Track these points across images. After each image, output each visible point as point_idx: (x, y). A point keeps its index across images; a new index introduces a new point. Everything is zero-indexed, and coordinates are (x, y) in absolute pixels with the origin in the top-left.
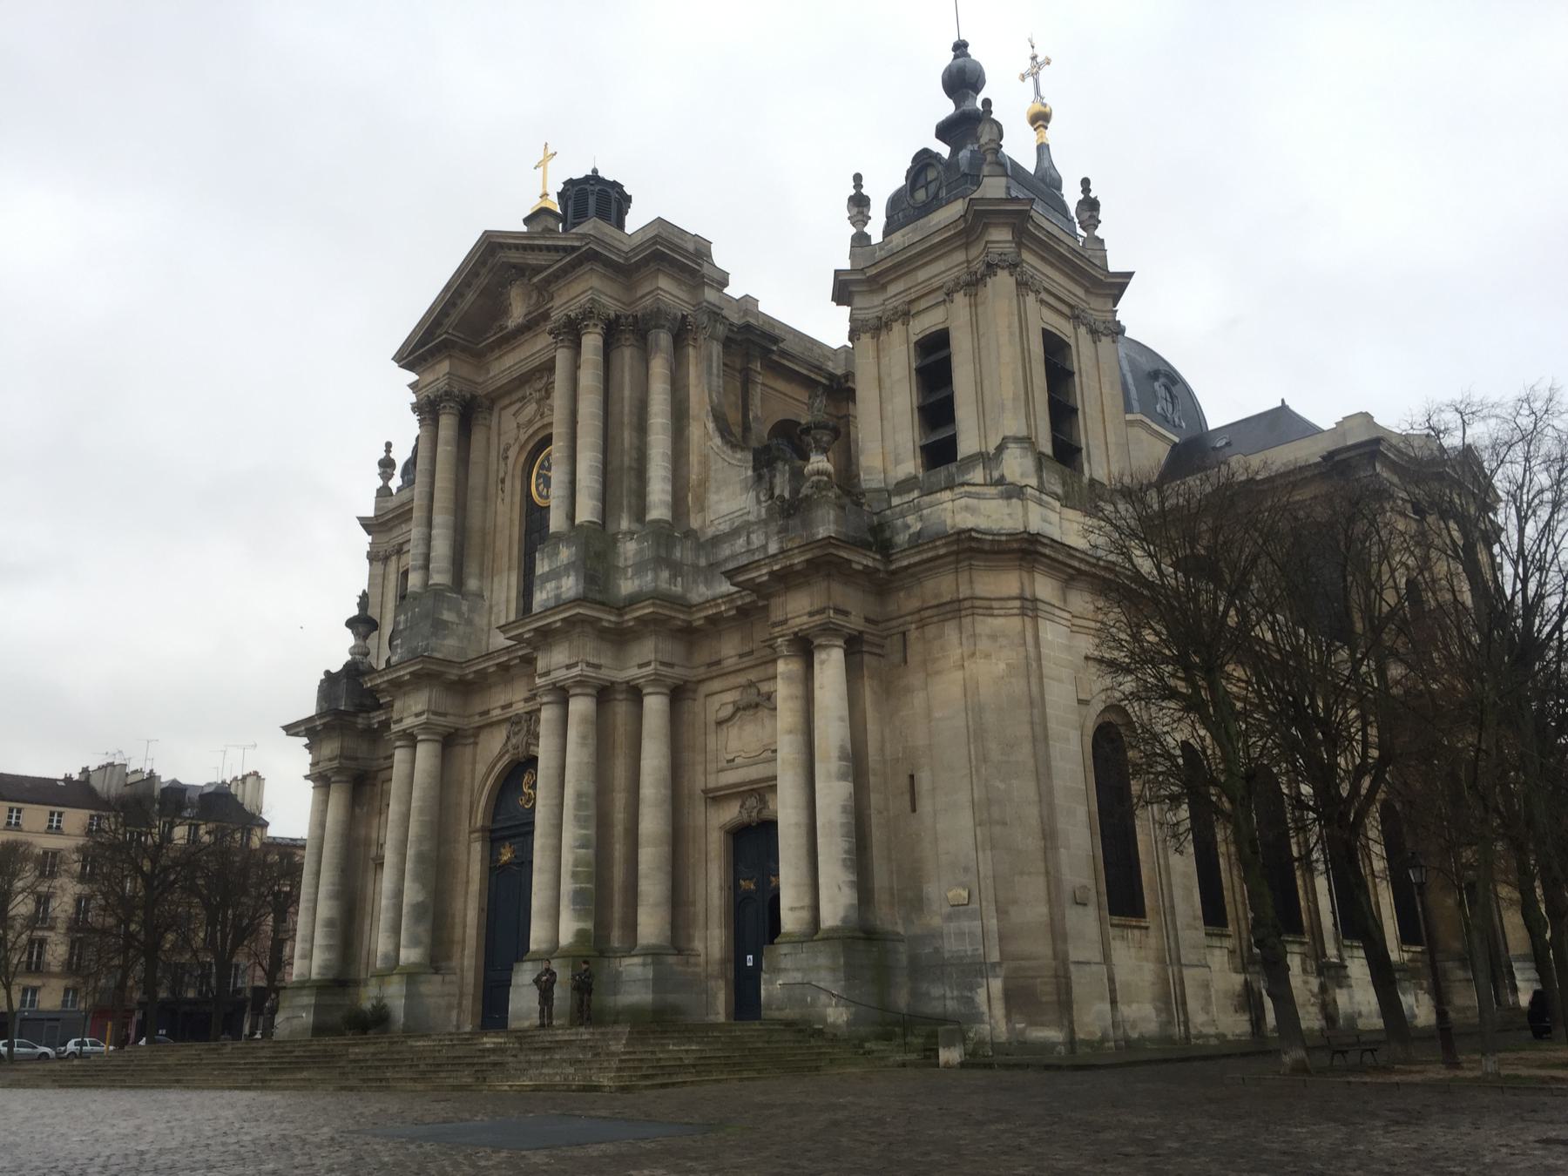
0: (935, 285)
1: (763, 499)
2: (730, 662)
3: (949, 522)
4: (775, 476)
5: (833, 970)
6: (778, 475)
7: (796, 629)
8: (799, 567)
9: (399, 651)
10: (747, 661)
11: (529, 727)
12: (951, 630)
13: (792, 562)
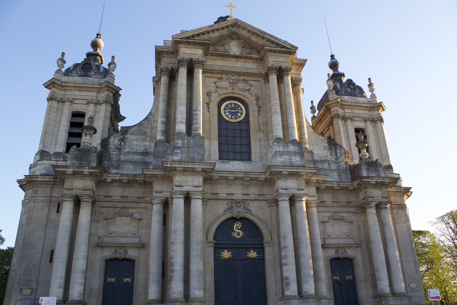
0: (361, 116)
1: (333, 155)
2: (329, 203)
4: (337, 150)
6: (338, 149)
7: (381, 201)
8: (386, 183)
9: (179, 155)
10: (336, 204)
13: (385, 181)
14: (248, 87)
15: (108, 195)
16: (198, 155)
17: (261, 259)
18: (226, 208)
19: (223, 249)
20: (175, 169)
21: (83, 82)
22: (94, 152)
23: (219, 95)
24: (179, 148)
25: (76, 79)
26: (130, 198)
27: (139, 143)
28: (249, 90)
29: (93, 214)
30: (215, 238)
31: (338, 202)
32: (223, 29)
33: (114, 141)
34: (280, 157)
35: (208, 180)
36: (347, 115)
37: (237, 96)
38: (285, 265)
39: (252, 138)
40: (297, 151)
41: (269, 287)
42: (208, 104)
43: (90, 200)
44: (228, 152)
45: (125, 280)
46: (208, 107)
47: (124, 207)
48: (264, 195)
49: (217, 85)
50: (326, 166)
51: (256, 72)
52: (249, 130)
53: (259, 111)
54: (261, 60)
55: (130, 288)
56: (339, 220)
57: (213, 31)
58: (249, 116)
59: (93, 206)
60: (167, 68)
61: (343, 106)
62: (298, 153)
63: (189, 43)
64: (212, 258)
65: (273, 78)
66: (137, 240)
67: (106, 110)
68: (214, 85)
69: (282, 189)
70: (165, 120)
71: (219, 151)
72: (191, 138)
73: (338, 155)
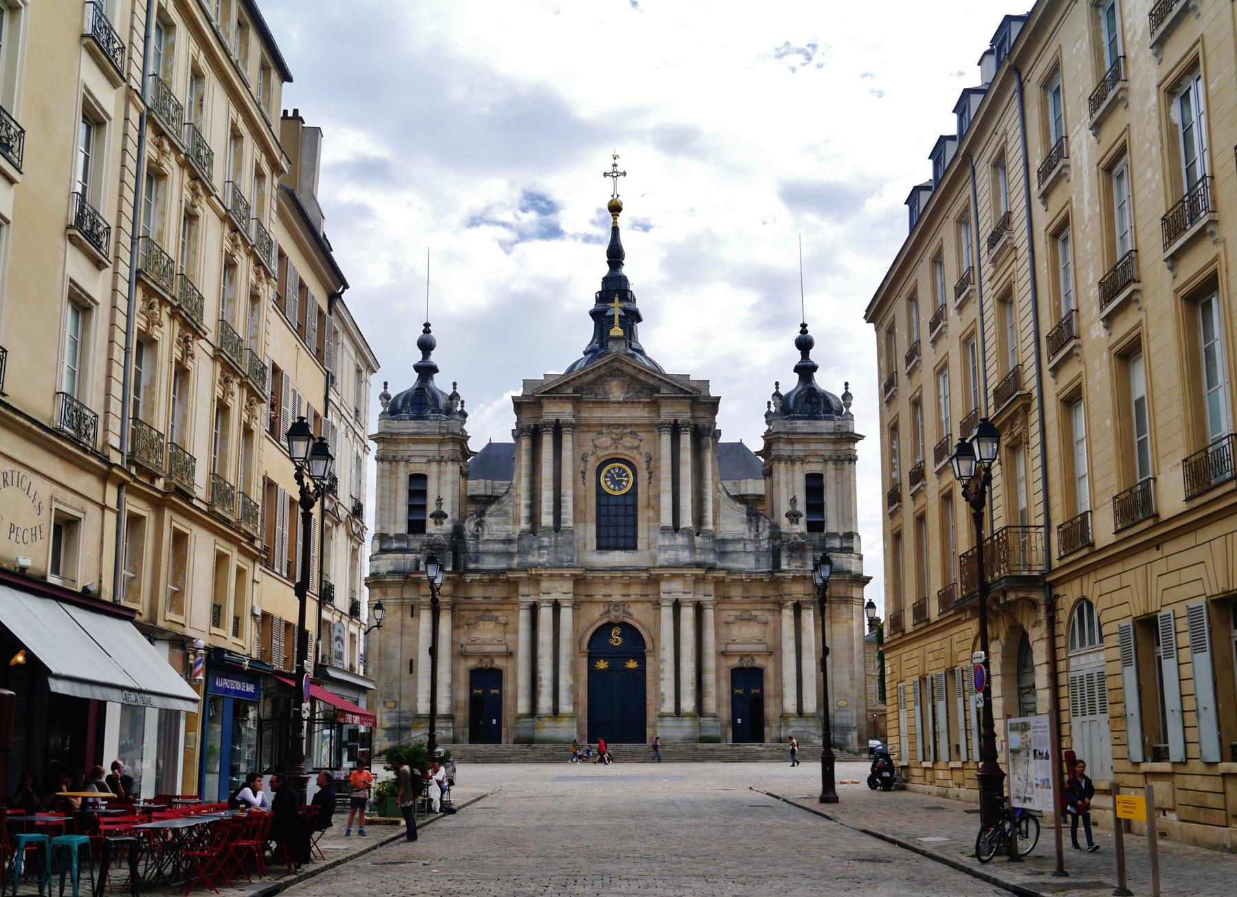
2: (737, 599)
3: (845, 566)
5: (817, 727)
9: (546, 557)
11: (624, 609)
12: (843, 607)
14: (636, 443)
15: (467, 596)
16: (567, 555)
17: (642, 670)
18: (602, 611)
19: (598, 659)
20: (541, 575)
21: (418, 428)
22: (449, 550)
23: (598, 459)
24: (545, 547)
25: (407, 426)
26: (493, 599)
27: (499, 527)
28: (637, 448)
29: (453, 619)
30: (589, 647)
31: (749, 597)
32: (600, 367)
33: (470, 526)
34: (665, 553)
35: (578, 581)
36: (796, 453)
37: (621, 457)
38: (662, 680)
39: (640, 517)
40: (687, 544)
41: (648, 702)
42: (583, 473)
43: (450, 607)
44: (609, 537)
45: (493, 691)
46: (584, 478)
47: (489, 610)
48: (647, 595)
49: (596, 442)
50: (740, 547)
51: (647, 422)
52: (637, 505)
53: (650, 478)
54: (655, 405)
55: (497, 702)
56: (749, 620)
57: (587, 374)
58: (637, 484)
59: (452, 611)
60: (529, 427)
61: (790, 442)
62: (688, 546)
63: (555, 398)
64: (586, 670)
65: (666, 439)
66: (502, 648)
67: (453, 472)
68: (591, 444)
69: (664, 593)
70: (529, 502)
71: (597, 537)
72: (559, 534)
73: (760, 530)
